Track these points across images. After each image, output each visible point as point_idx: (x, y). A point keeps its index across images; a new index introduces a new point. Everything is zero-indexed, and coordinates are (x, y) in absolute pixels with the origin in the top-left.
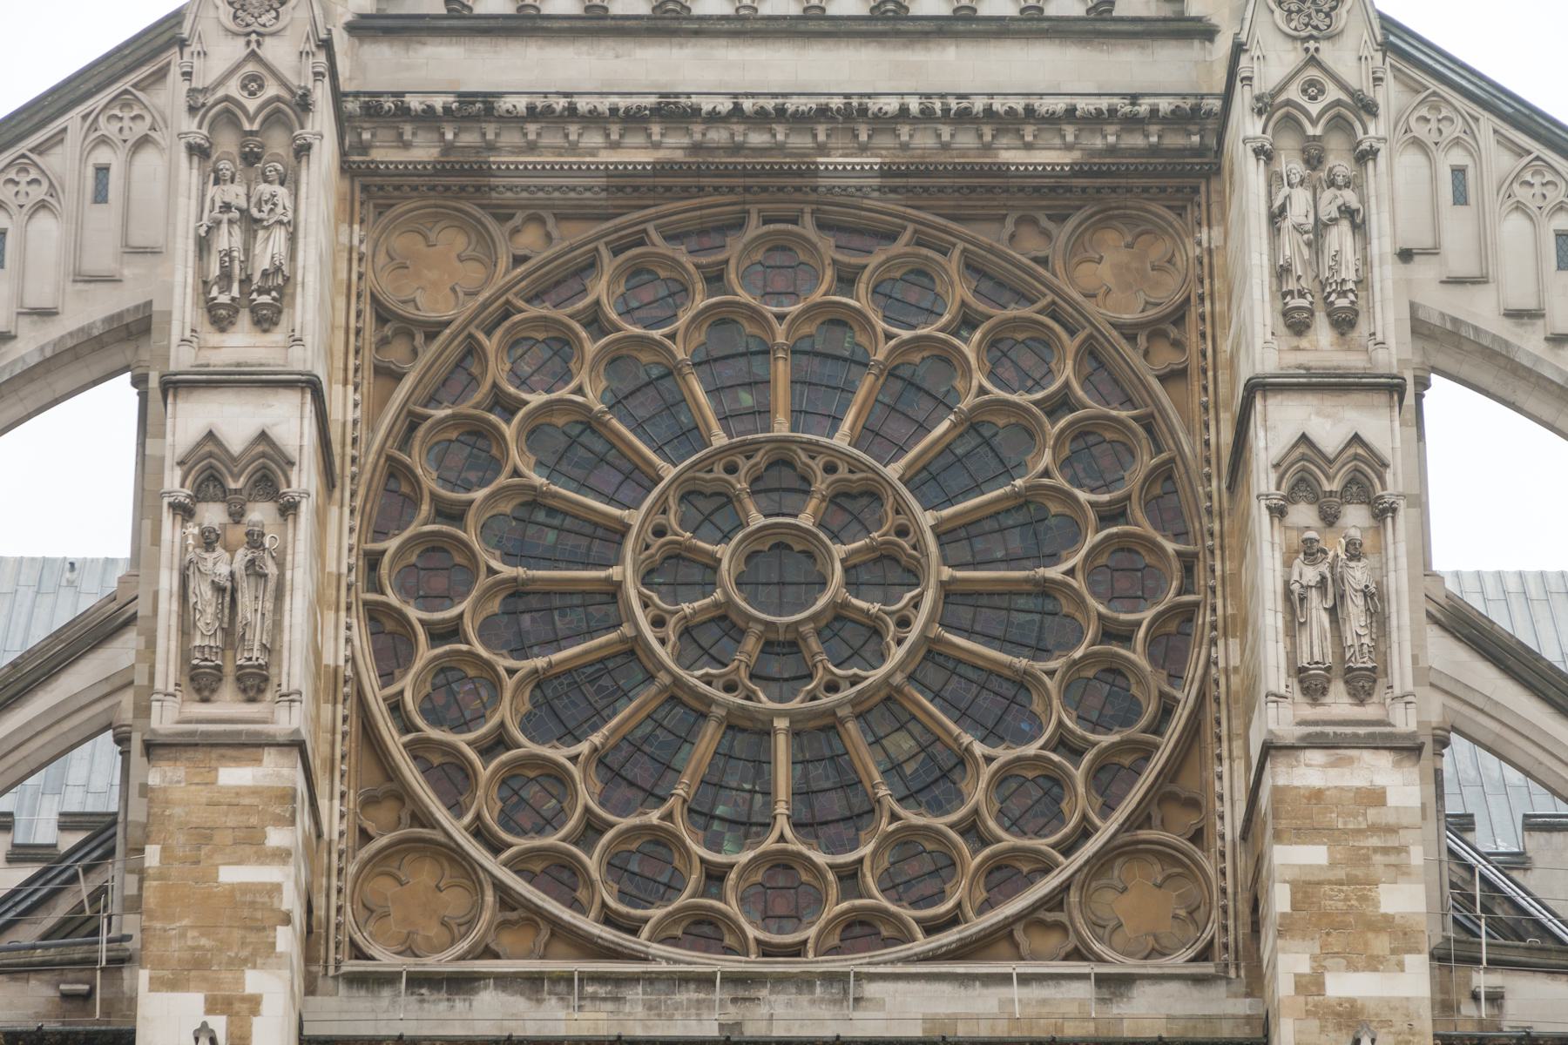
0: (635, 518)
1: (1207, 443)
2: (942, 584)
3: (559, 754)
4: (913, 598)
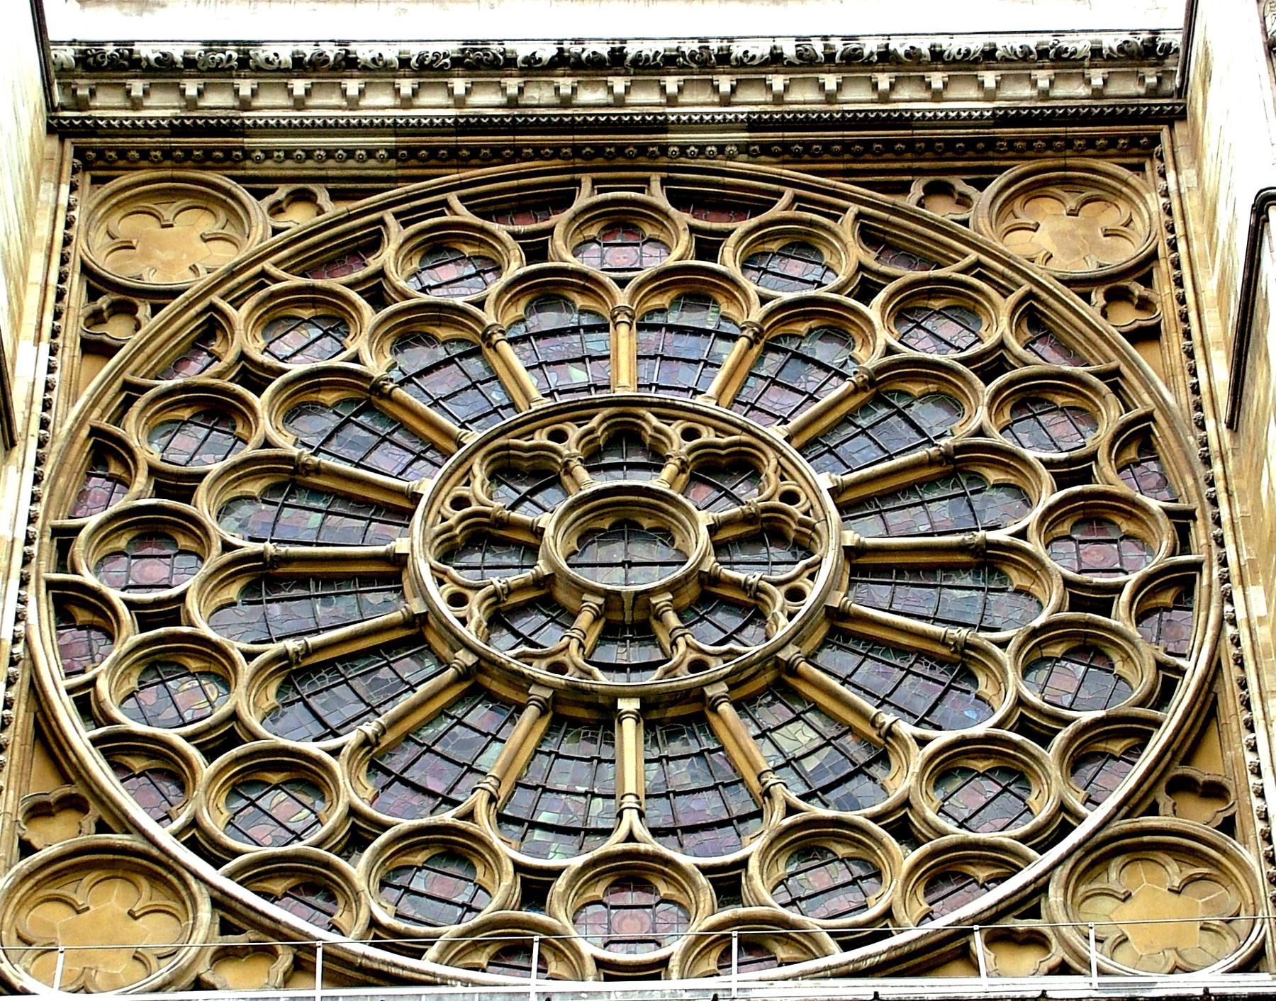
0: (426, 487)
1: (1196, 390)
4: (807, 567)
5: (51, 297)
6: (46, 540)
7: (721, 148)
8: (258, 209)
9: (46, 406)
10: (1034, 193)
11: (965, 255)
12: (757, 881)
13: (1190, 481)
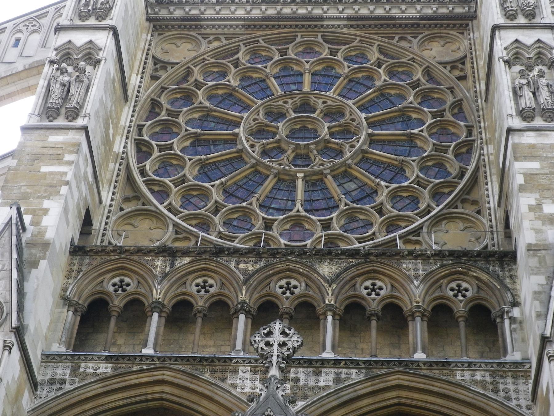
1: (476, 92)
2: (370, 135)
3: (207, 185)
4: (356, 139)
5: (143, 63)
6: (135, 128)
7: (339, 26)
8: (204, 42)
9: (138, 92)
10: (431, 40)
11: (409, 56)
12: (335, 224)
13: (473, 117)
